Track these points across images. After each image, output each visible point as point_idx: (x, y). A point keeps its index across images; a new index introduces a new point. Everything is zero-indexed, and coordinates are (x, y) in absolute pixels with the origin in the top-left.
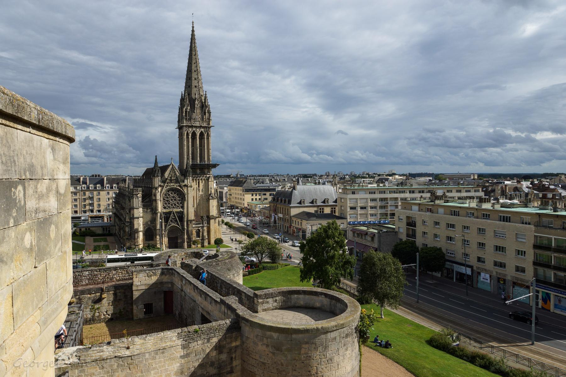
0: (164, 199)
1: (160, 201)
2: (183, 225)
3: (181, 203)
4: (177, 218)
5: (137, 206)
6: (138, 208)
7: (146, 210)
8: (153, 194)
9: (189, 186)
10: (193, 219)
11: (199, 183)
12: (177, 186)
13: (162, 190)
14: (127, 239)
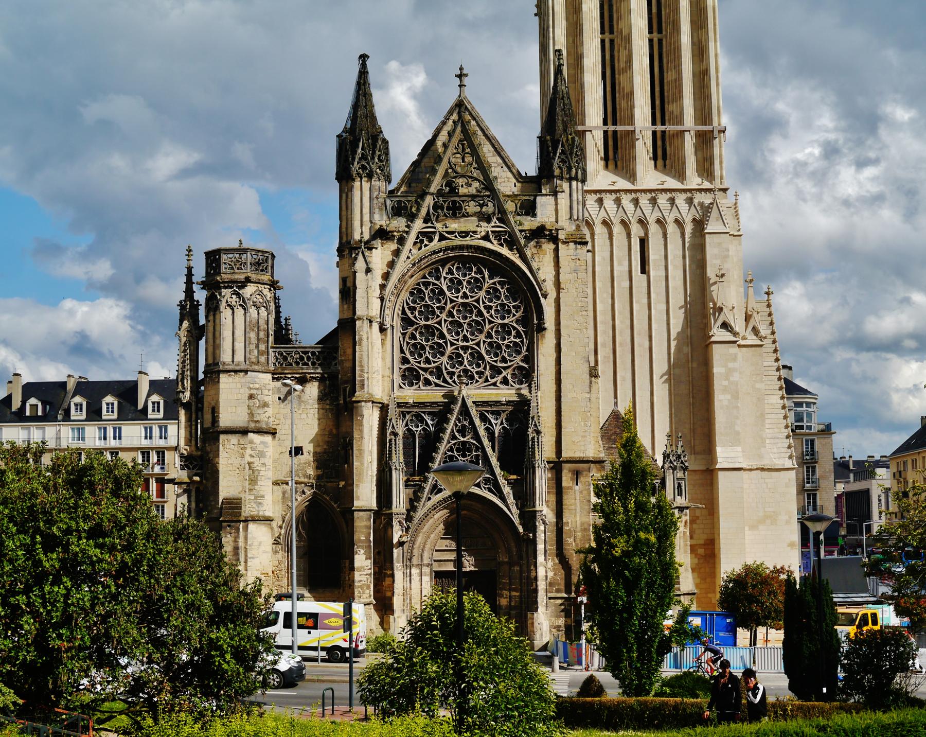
0: (407, 322)
1: (382, 330)
2: (525, 495)
3: (516, 348)
5: (240, 357)
6: (246, 372)
9: (562, 236)
11: (643, 243)
12: (486, 238)
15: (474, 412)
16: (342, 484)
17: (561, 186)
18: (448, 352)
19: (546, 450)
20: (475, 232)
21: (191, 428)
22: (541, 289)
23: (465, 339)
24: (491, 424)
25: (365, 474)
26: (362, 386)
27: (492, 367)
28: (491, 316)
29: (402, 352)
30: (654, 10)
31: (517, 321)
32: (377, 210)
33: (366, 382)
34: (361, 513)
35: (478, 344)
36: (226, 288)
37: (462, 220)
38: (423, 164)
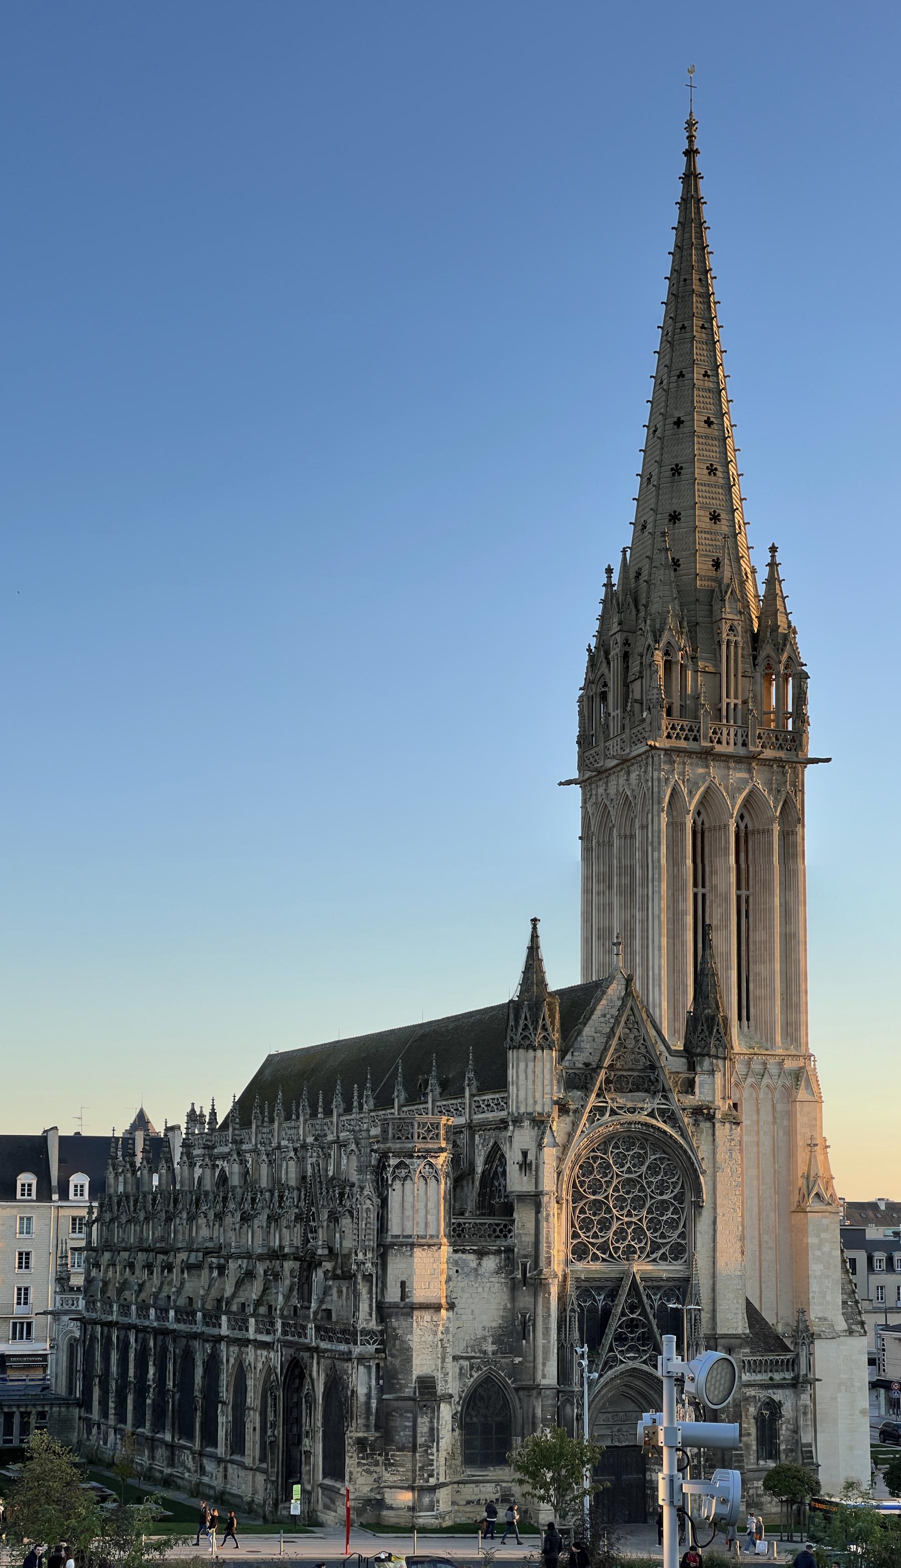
0: (577, 1197)
4: (654, 1322)
6: (440, 1245)
7: (471, 1259)
8: (513, 1156)
9: (718, 1116)
10: (740, 1331)
12: (651, 1115)
13: (570, 1135)
14: (361, 1444)
15: (641, 1288)
16: (517, 1360)
17: (718, 1065)
18: (614, 1228)
19: (704, 1329)
20: (642, 1109)
21: (371, 1301)
22: (701, 1167)
23: (629, 1215)
24: (652, 1301)
25: (551, 1352)
26: (549, 1264)
27: (652, 1241)
28: (652, 1191)
29: (573, 1226)
30: (743, 866)
31: (675, 1198)
32: (555, 1082)
33: (552, 1259)
34: (548, 1392)
35: (640, 1220)
36: (418, 1157)
37: (629, 1094)
38: (584, 1033)
